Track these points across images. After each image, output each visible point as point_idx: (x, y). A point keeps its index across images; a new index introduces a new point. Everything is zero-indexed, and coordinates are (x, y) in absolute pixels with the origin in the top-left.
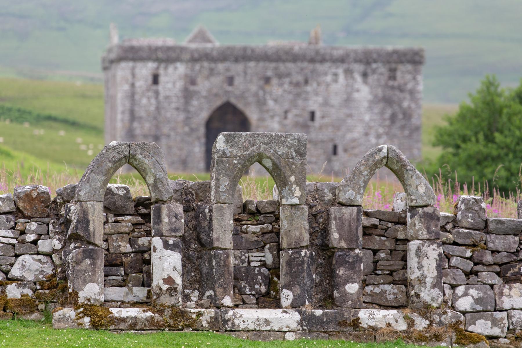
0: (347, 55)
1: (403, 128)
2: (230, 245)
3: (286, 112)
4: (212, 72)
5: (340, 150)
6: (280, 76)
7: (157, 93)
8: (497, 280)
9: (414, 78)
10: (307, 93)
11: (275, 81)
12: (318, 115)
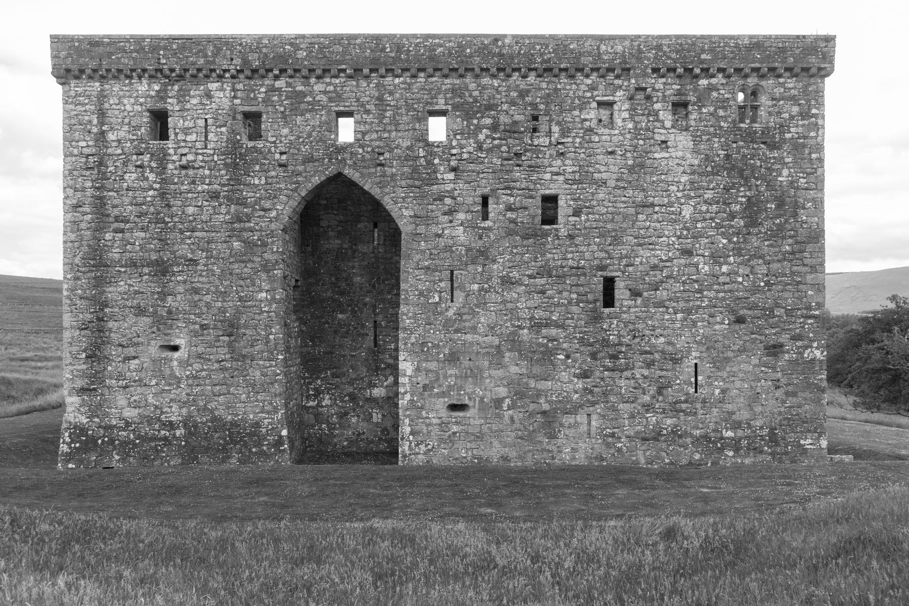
0: (639, 55)
5: (621, 292)
7: (162, 158)
9: (805, 115)
10: (537, 149)
12: (564, 206)
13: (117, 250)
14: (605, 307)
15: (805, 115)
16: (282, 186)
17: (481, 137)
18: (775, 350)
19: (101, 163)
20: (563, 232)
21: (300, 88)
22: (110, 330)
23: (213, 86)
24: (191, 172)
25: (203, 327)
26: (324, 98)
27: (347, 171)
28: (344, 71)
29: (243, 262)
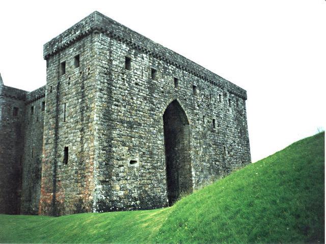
3: (204, 117)
4: (165, 72)
13: (116, 114)
16: (163, 100)
19: (110, 74)
21: (166, 66)
22: (114, 152)
23: (144, 55)
24: (138, 87)
25: (144, 153)
27: (178, 99)
28: (176, 64)
29: (154, 127)
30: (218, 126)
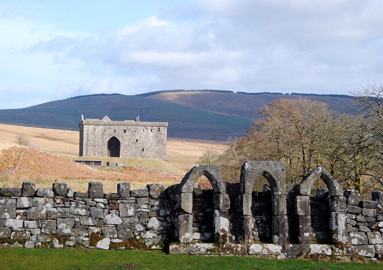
1: (161, 144)
2: (251, 214)
3: (130, 139)
4: (110, 128)
6: (128, 130)
8: (368, 230)
11: (127, 131)
14: (143, 151)
15: (164, 131)
17: (130, 133)
18: (161, 156)
20: (138, 143)
23: (100, 126)
26: (113, 128)
30: (140, 141)
